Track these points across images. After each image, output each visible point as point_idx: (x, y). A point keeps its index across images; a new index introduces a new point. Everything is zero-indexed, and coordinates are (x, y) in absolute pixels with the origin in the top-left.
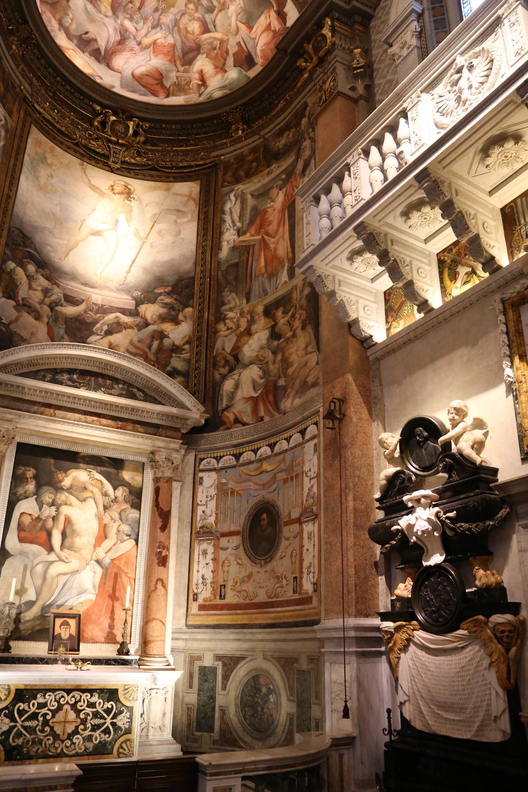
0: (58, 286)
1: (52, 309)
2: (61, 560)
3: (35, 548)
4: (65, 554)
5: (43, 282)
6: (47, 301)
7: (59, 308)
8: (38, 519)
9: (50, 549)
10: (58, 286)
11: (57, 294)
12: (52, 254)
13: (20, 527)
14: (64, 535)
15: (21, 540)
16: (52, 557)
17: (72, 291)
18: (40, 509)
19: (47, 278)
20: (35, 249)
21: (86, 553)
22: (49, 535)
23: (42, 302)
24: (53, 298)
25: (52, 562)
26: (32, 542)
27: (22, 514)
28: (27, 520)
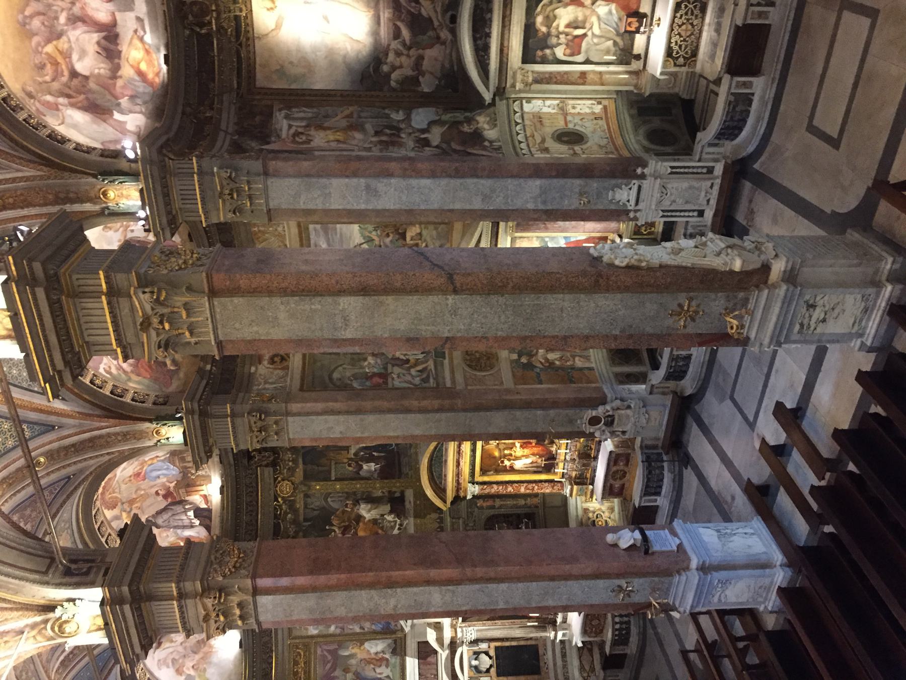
0: (389, 45)
1: (409, 48)
2: (591, 28)
3: (584, 45)
4: (588, 25)
5: (391, 57)
6: (405, 52)
7: (408, 42)
8: (567, 45)
9: (585, 35)
10: (389, 45)
11: (395, 45)
12: (364, 53)
13: (572, 55)
14: (576, 28)
15: (579, 53)
16: (589, 33)
17: (388, 34)
18: (560, 44)
19: (387, 55)
20: (369, 66)
21: (588, 12)
22: (576, 37)
23: (408, 56)
24: (401, 48)
25: (593, 34)
26: (580, 47)
27: (564, 55)
28: (568, 51)
